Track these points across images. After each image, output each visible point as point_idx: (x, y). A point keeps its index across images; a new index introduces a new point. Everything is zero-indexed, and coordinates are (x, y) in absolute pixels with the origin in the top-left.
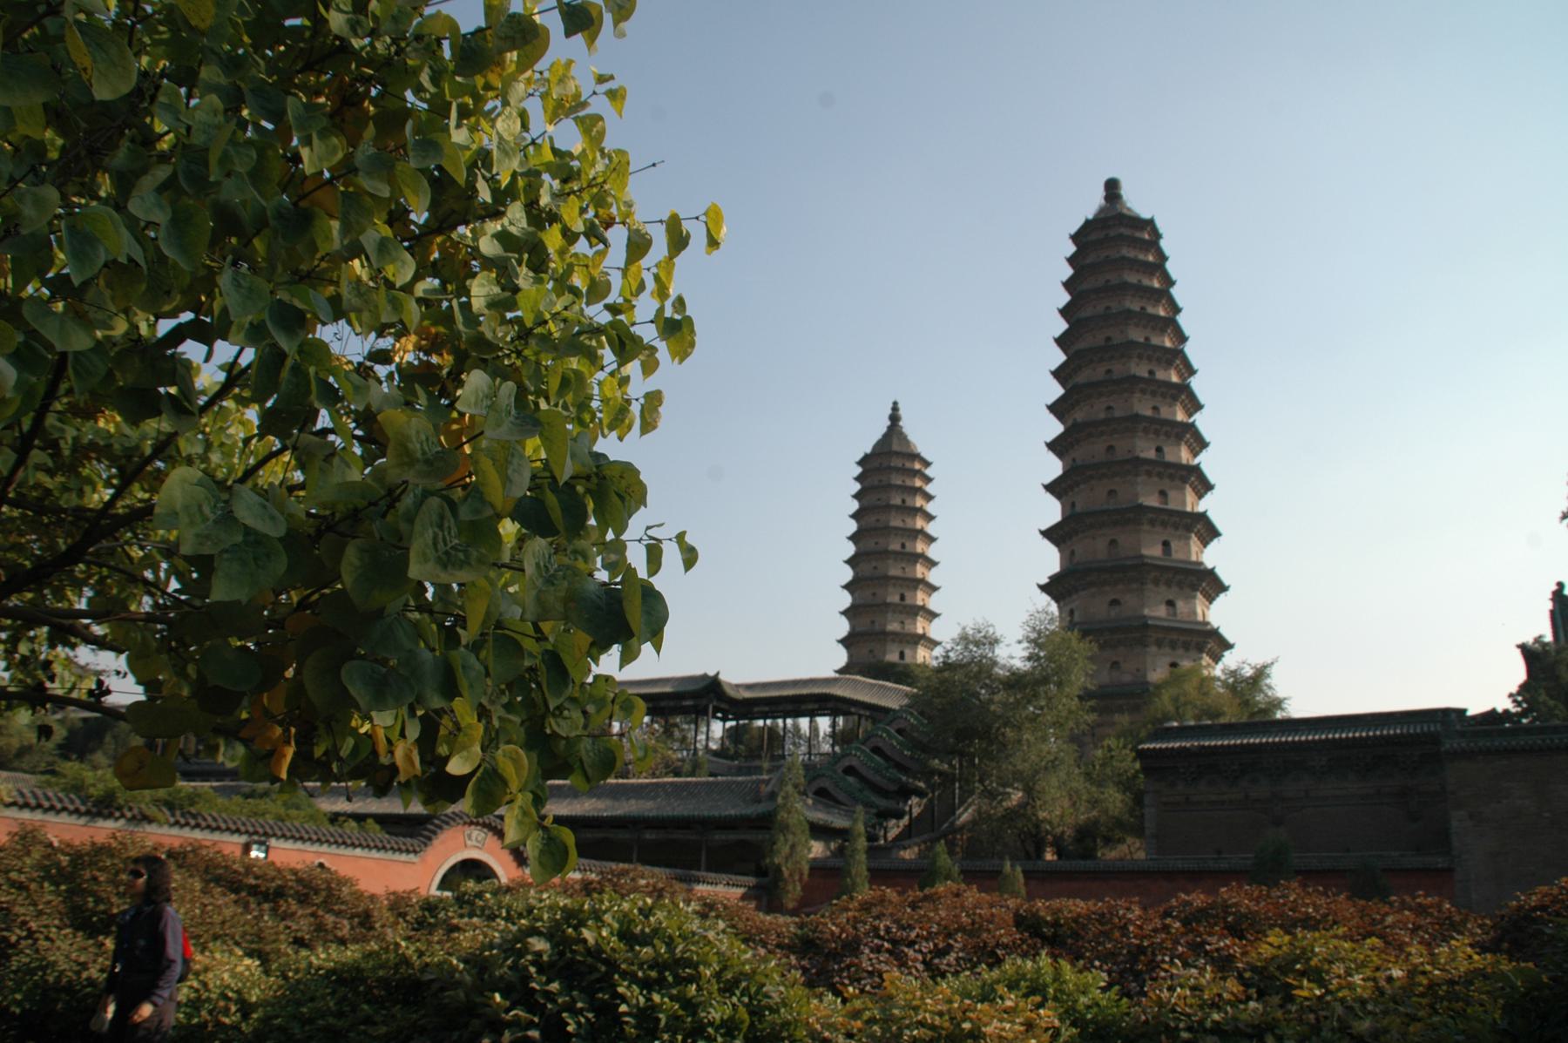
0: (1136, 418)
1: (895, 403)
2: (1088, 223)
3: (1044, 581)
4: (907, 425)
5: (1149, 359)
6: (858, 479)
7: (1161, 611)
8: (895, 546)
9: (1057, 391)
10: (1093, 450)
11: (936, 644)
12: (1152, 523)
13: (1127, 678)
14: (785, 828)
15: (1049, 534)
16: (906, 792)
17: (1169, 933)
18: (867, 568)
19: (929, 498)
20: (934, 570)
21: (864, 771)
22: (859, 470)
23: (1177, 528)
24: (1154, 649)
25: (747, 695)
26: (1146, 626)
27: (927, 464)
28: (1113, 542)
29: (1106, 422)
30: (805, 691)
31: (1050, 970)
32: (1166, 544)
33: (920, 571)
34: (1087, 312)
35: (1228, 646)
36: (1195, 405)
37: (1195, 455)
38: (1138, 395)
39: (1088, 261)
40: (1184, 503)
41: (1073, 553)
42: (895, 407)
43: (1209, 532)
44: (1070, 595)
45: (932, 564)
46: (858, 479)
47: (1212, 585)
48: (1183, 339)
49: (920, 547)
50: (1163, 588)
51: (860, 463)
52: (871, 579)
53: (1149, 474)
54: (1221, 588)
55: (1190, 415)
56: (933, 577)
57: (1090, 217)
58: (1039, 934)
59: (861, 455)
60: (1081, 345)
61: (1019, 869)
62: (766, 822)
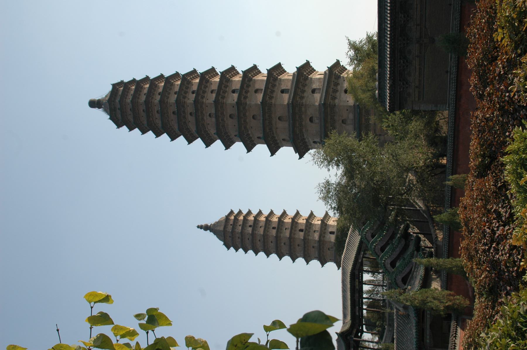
0: (216, 102)
1: (198, 227)
2: (111, 118)
3: (297, 155)
4: (210, 221)
5: (186, 93)
6: (237, 250)
7: (317, 96)
8: (274, 232)
9: (199, 142)
10: (231, 125)
11: (327, 214)
12: (271, 98)
13: (351, 116)
14: (424, 302)
15: (273, 152)
16: (406, 235)
17: (493, 94)
18: (284, 248)
19: (249, 213)
20: (288, 213)
21: (394, 257)
22: (232, 249)
23: (275, 85)
25: (349, 318)
26: (324, 104)
27: (232, 212)
28: (280, 118)
29: (217, 117)
30: (349, 286)
31: (511, 156)
32: (283, 91)
33: (288, 220)
34: (159, 123)
35: (338, 62)
36: (212, 71)
37: (238, 73)
38: (204, 100)
39: (132, 120)
40: (263, 80)
41: (284, 140)
42: (200, 227)
43: (278, 69)
44: (306, 142)
45: (284, 213)
46: (237, 250)
47: (306, 69)
48: (177, 74)
49: (275, 219)
50: (305, 94)
51: (228, 248)
52: (290, 246)
53: (246, 98)
54: (308, 63)
55: (217, 74)
56: (291, 213)
57: (109, 117)
58: (490, 163)
59: (224, 248)
60: (176, 127)
61: (451, 177)
62: (420, 312)
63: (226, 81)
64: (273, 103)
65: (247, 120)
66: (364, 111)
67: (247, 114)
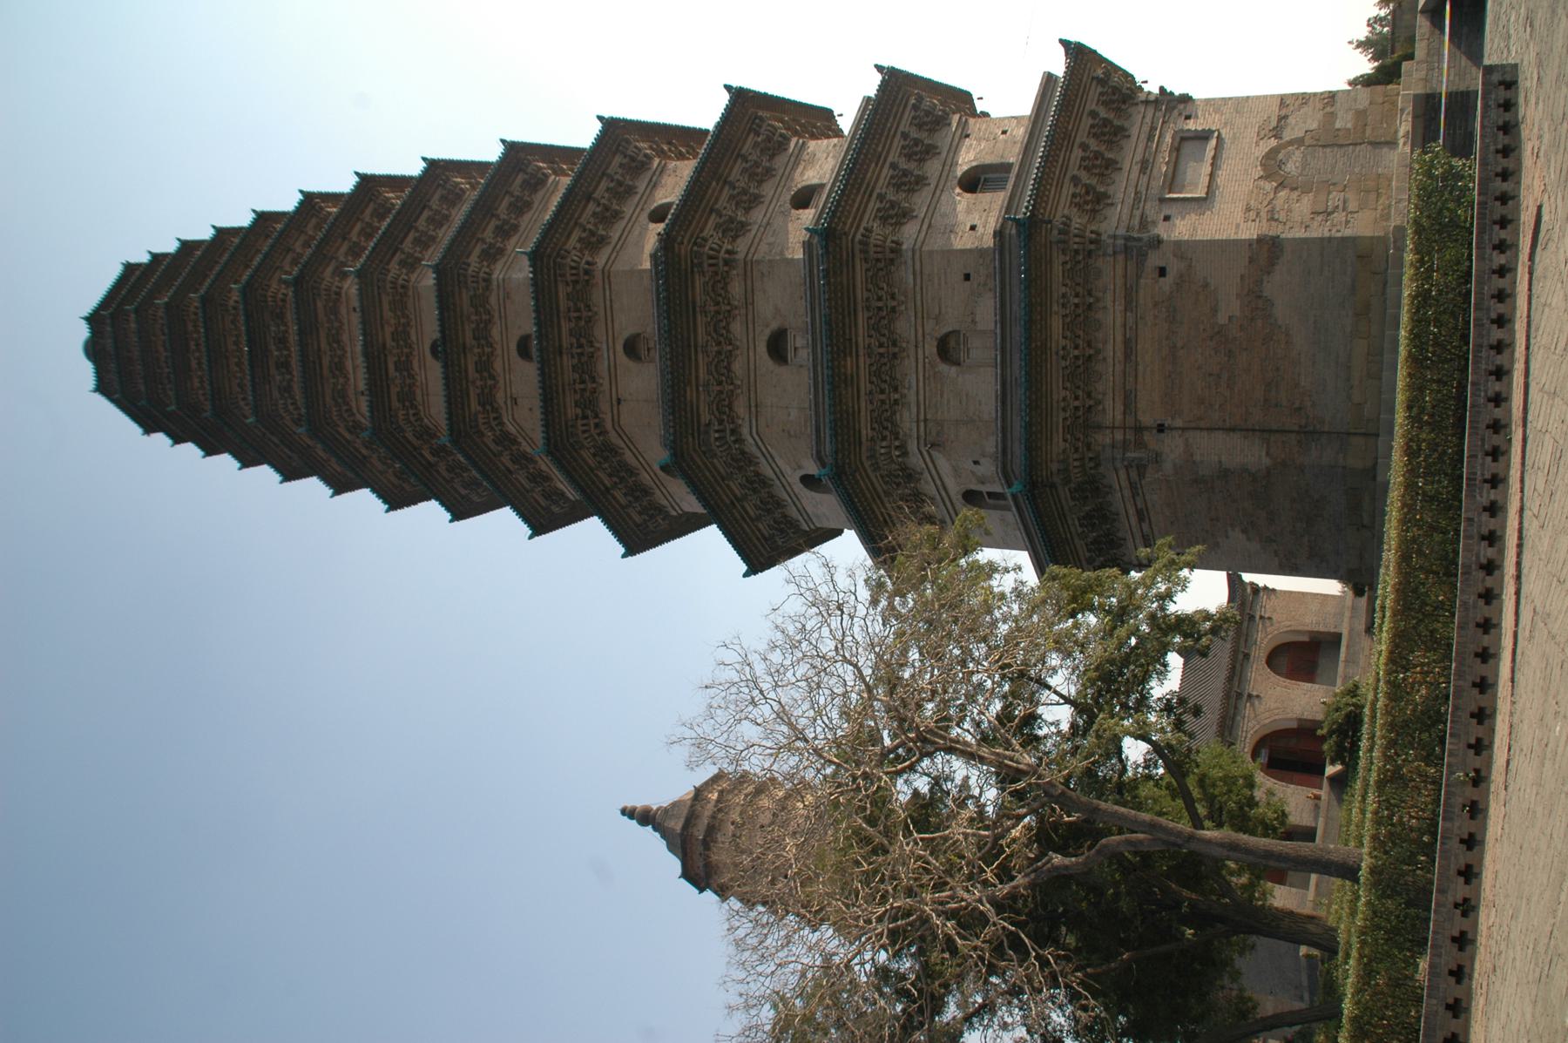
4: (658, 798)
12: (594, 243)
13: (986, 312)
23: (631, 191)
24: (909, 232)
42: (629, 813)
50: (757, 215)
63: (443, 198)
65: (498, 365)
66: (1058, 269)
67: (495, 332)
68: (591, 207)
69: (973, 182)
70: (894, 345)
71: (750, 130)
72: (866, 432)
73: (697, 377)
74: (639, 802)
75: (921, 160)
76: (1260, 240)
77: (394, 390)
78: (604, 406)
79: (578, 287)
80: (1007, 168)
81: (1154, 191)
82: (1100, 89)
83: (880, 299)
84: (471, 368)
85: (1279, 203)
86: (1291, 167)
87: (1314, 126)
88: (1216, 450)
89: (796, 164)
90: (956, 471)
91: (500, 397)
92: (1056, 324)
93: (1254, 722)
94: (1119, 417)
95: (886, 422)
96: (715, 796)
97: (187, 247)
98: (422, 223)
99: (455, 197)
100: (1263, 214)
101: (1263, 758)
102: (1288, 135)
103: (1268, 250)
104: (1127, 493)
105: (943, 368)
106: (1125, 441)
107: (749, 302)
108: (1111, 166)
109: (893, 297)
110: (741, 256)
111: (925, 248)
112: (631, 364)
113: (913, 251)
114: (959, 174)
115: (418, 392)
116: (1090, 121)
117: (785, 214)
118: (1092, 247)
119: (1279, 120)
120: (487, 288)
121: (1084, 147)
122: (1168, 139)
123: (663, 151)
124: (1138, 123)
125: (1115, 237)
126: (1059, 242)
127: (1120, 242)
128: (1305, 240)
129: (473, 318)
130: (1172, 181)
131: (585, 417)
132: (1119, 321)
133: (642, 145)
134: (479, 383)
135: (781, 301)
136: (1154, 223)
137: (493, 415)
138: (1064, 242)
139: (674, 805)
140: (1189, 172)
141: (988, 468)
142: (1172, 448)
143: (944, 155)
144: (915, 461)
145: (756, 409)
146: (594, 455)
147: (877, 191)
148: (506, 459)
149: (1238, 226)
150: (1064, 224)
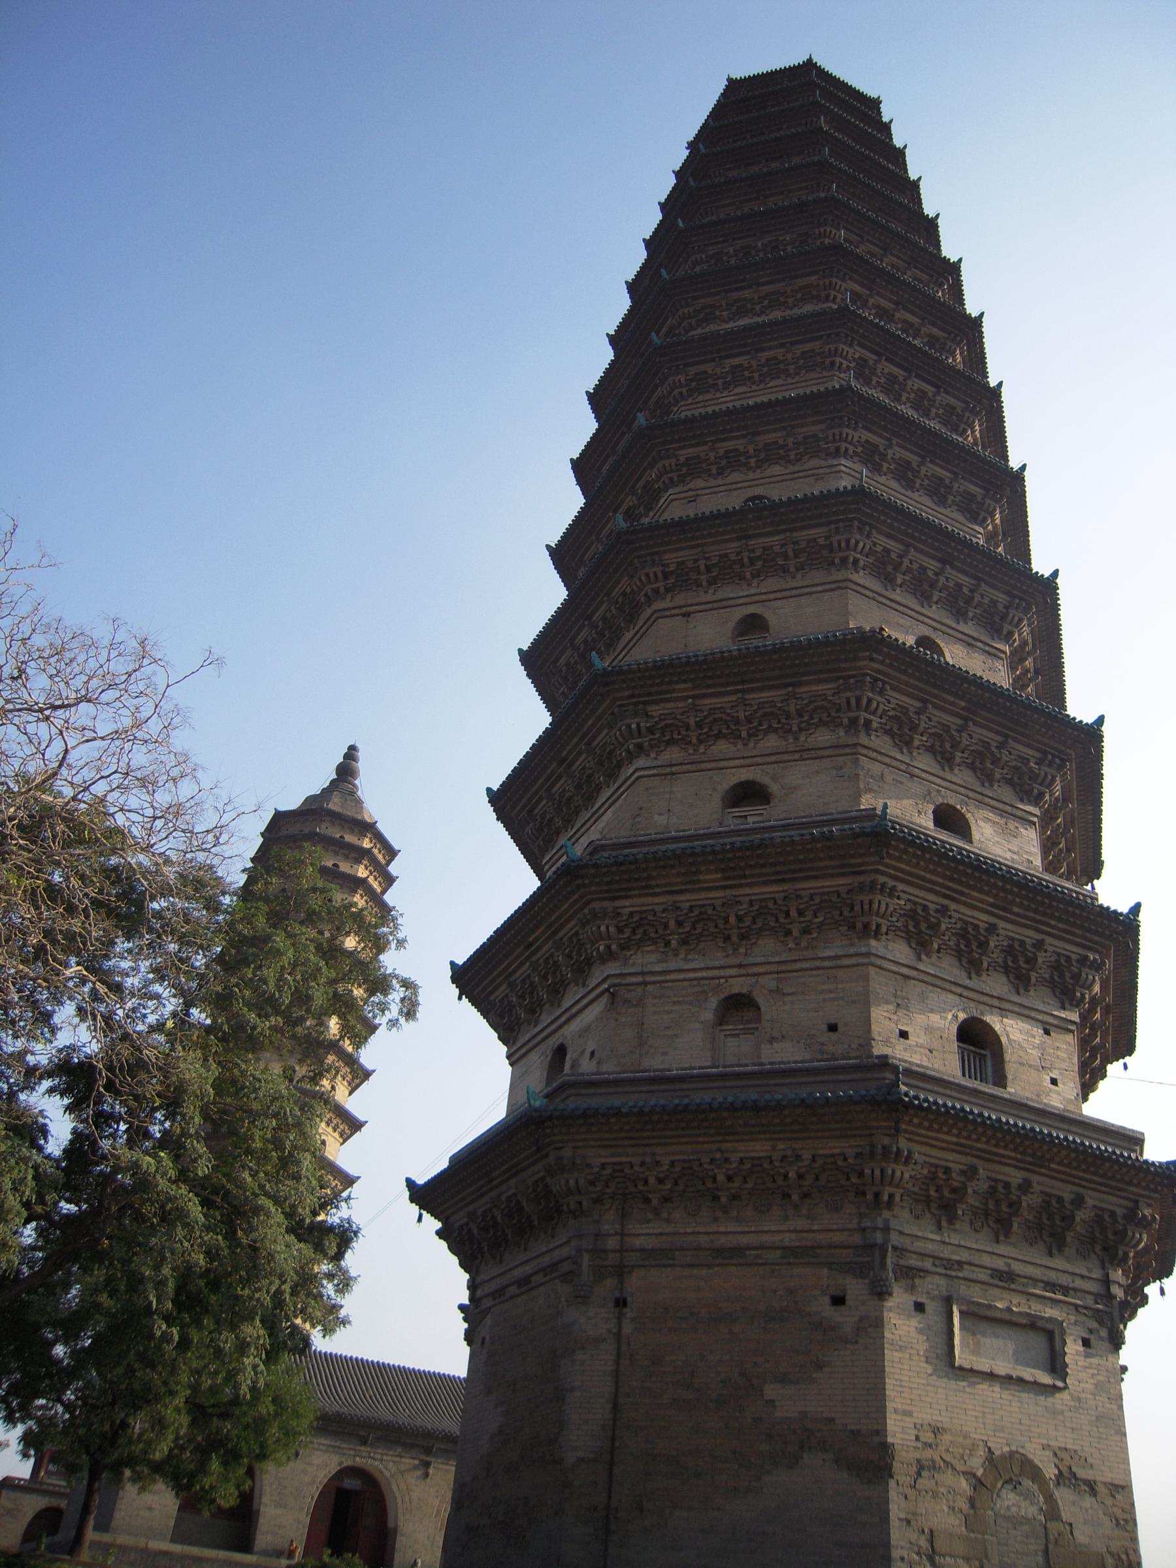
1: (352, 748)
23: (960, 614)
24: (899, 951)
27: (392, 853)
42: (351, 754)
50: (924, 762)
64: (855, 577)
65: (736, 476)
66: (836, 1147)
67: (776, 469)
68: (932, 565)
69: (976, 1039)
70: (743, 937)
71: (1045, 753)
72: (626, 906)
73: (704, 696)
74: (363, 765)
75: (1006, 970)
76: (885, 1449)
77: (708, 367)
78: (680, 599)
79: (825, 553)
80: (1000, 1080)
81: (963, 1290)
82: (1120, 1212)
83: (801, 913)
84: (730, 445)
85: (948, 1478)
86: (1008, 1500)
87: (1081, 1536)
88: (590, 1379)
89: (1002, 813)
90: (585, 1031)
91: (699, 483)
92: (758, 1148)
93: (392, 1468)
94: (638, 1243)
95: (641, 932)
96: (366, 844)
97: (899, 156)
98: (915, 383)
99: (957, 422)
100: (928, 1454)
101: (349, 1483)
102: (1063, 1496)
103: (871, 1459)
104: (546, 1260)
105: (713, 1002)
106: (605, 1251)
107: (805, 754)
108: (1001, 1228)
109: (806, 931)
110: (863, 739)
111: (872, 971)
112: (731, 625)
113: (868, 954)
114: (988, 1019)
115: (708, 396)
116: (1067, 1197)
117: (927, 796)
118: (870, 1197)
119: (1087, 1483)
120: (829, 455)
121: (1025, 1186)
122: (1050, 1312)
123: (1022, 660)
124: (1076, 1270)
125: (887, 1229)
126: (873, 1146)
127: (879, 1237)
128: (885, 1519)
129: (791, 440)
130: (977, 1317)
131: (666, 576)
132: (767, 1239)
133: (1026, 630)
134: (712, 455)
135: (806, 791)
136: (912, 1289)
137: (675, 476)
138: (872, 1154)
139: (359, 803)
140: (998, 1343)
141: (587, 1066)
142: (593, 1320)
143: (1015, 998)
144: (598, 973)
145: (669, 773)
146: (624, 594)
147: (953, 906)
148: (630, 501)
149: (909, 1414)
150: (899, 1152)
